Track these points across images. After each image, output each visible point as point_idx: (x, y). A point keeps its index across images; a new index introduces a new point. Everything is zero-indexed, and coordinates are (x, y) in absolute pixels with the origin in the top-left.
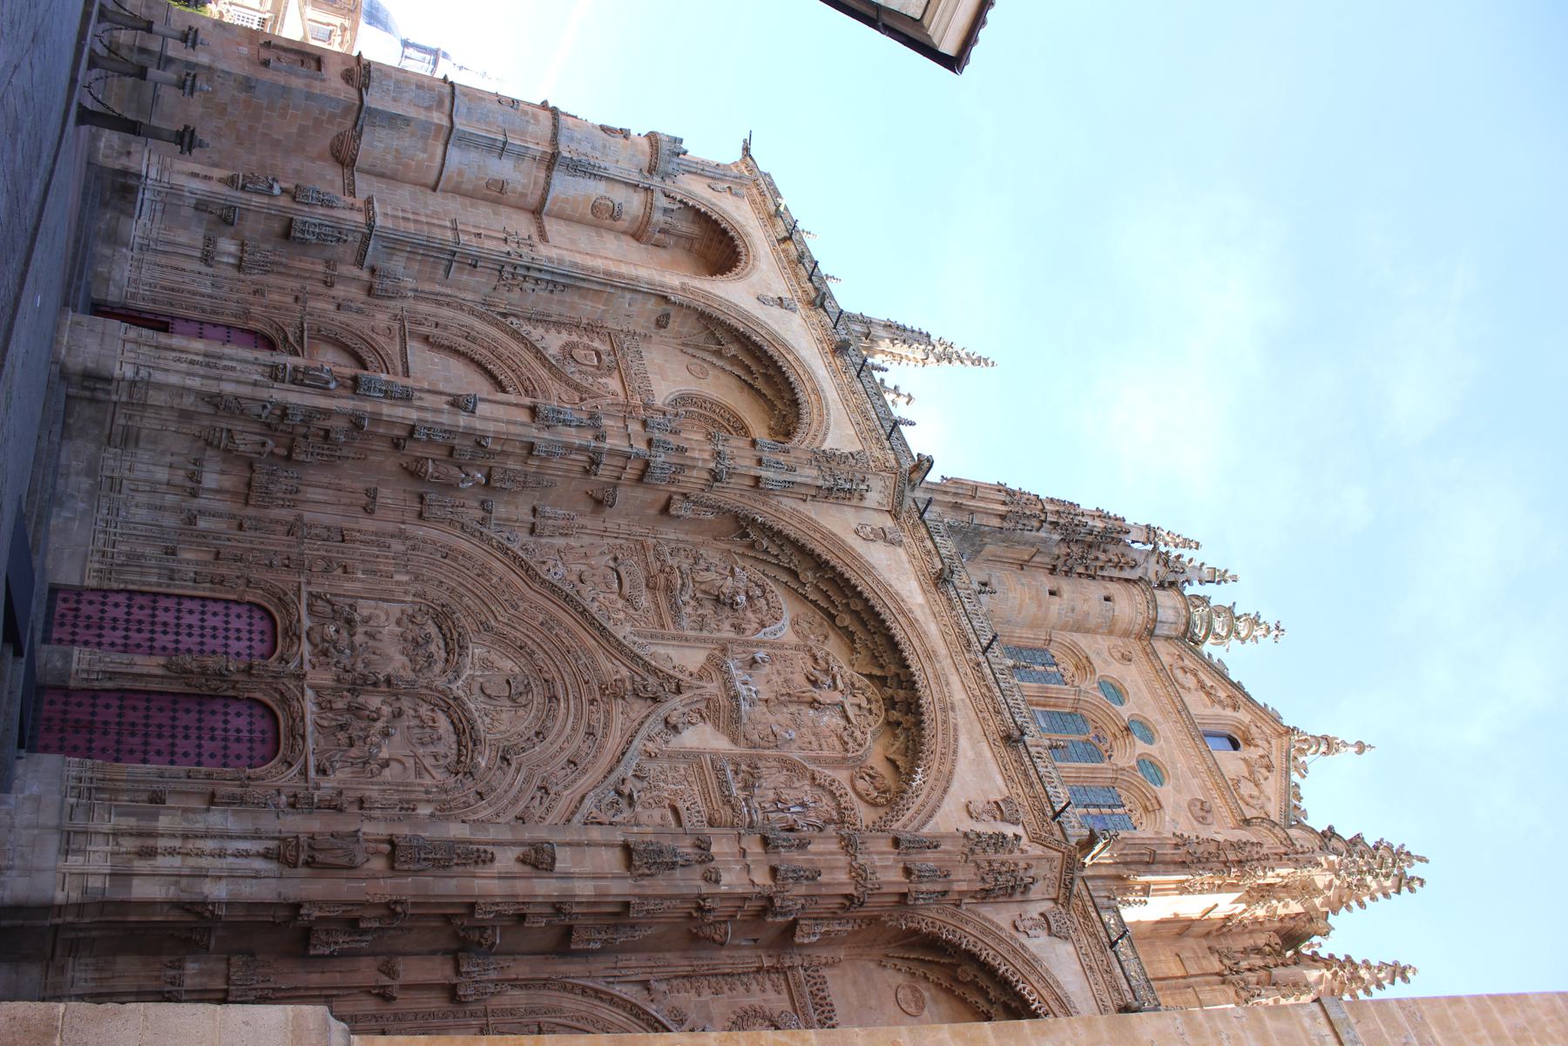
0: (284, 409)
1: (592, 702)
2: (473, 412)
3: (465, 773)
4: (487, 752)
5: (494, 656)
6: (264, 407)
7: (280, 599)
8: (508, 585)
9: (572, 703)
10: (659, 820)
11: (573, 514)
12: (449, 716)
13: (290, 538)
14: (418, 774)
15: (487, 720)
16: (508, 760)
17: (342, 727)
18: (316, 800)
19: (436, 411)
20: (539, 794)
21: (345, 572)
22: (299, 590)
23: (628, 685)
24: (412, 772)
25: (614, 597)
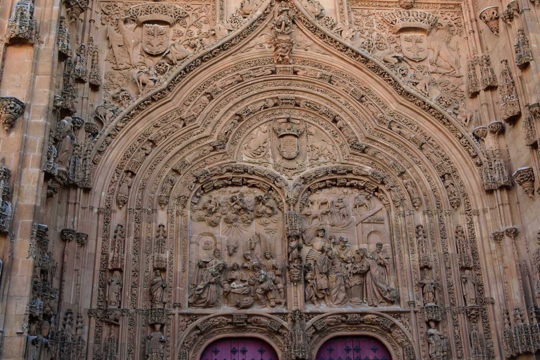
0: (32, 319)
1: (295, 73)
2: (23, 107)
3: (383, 183)
4: (356, 163)
5: (253, 145)
6: (34, 342)
7: (199, 335)
8: (165, 121)
9: (298, 88)
10: (410, 45)
11: (77, 46)
12: (315, 191)
13: (120, 323)
14: (380, 221)
15: (322, 159)
16: (366, 147)
17: (345, 282)
18: (433, 304)
19: (24, 145)
20: (394, 128)
21: (163, 270)
22: (188, 315)
23: (284, 38)
24: (379, 227)
25: (171, 32)
